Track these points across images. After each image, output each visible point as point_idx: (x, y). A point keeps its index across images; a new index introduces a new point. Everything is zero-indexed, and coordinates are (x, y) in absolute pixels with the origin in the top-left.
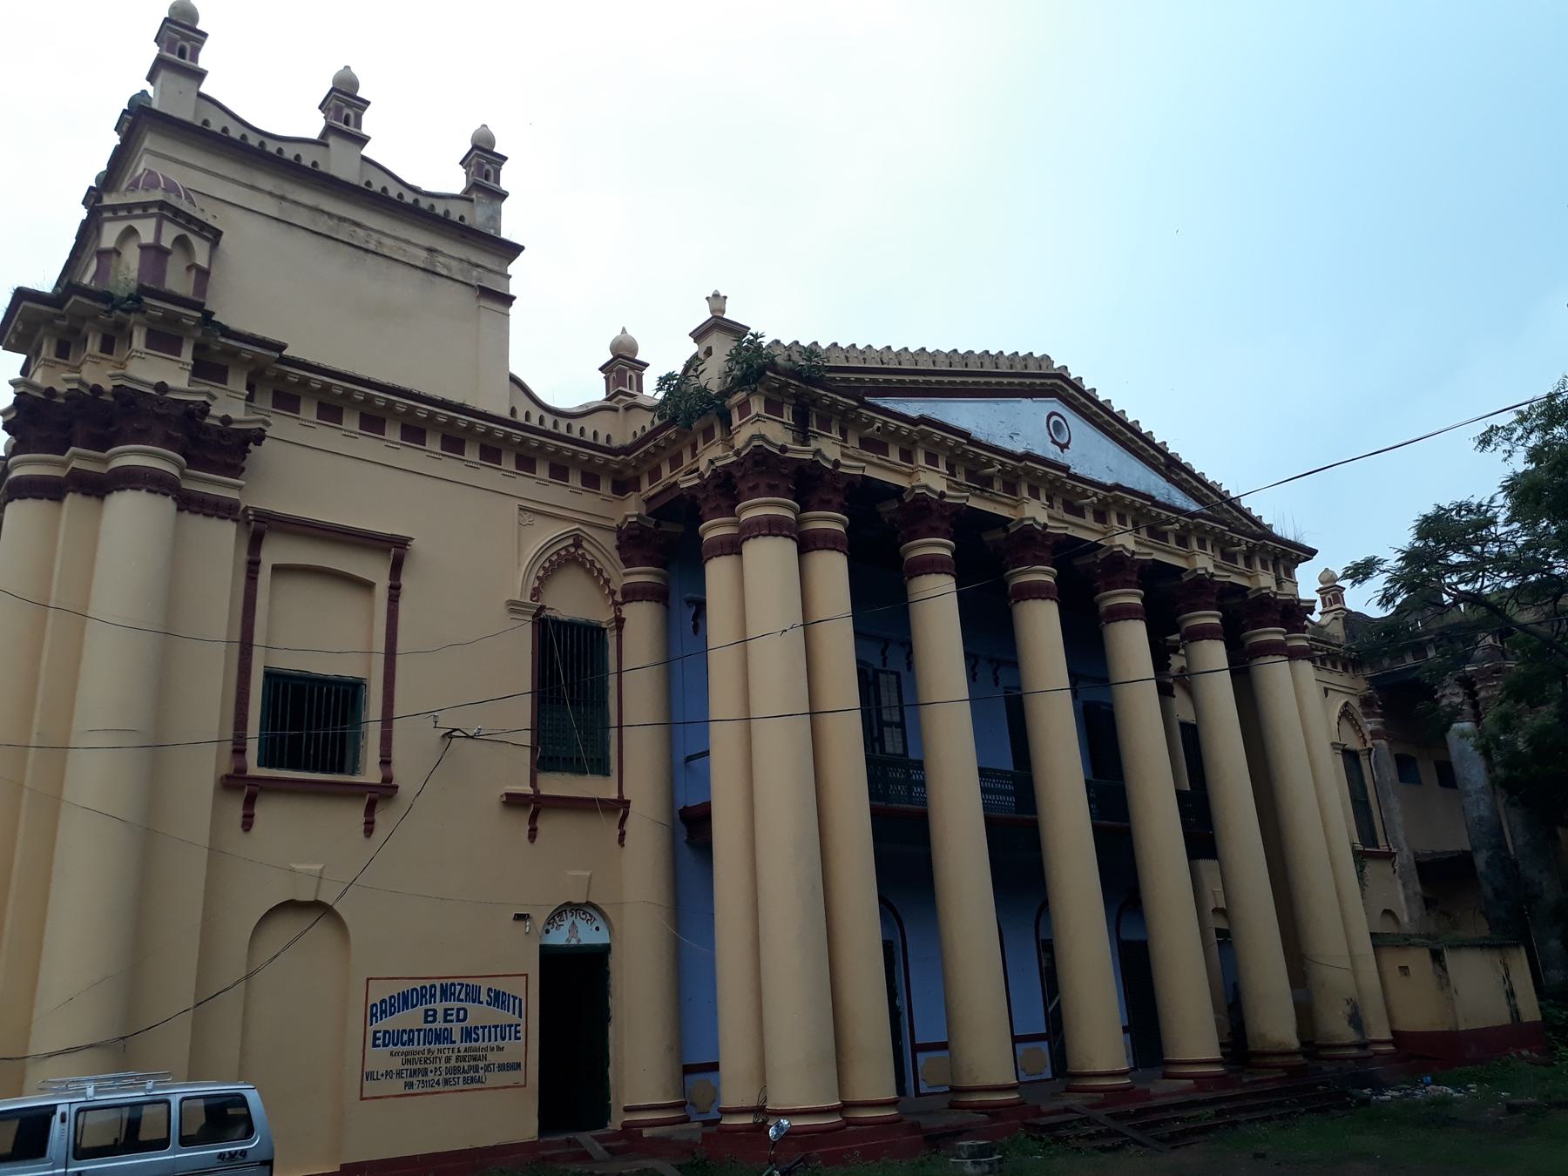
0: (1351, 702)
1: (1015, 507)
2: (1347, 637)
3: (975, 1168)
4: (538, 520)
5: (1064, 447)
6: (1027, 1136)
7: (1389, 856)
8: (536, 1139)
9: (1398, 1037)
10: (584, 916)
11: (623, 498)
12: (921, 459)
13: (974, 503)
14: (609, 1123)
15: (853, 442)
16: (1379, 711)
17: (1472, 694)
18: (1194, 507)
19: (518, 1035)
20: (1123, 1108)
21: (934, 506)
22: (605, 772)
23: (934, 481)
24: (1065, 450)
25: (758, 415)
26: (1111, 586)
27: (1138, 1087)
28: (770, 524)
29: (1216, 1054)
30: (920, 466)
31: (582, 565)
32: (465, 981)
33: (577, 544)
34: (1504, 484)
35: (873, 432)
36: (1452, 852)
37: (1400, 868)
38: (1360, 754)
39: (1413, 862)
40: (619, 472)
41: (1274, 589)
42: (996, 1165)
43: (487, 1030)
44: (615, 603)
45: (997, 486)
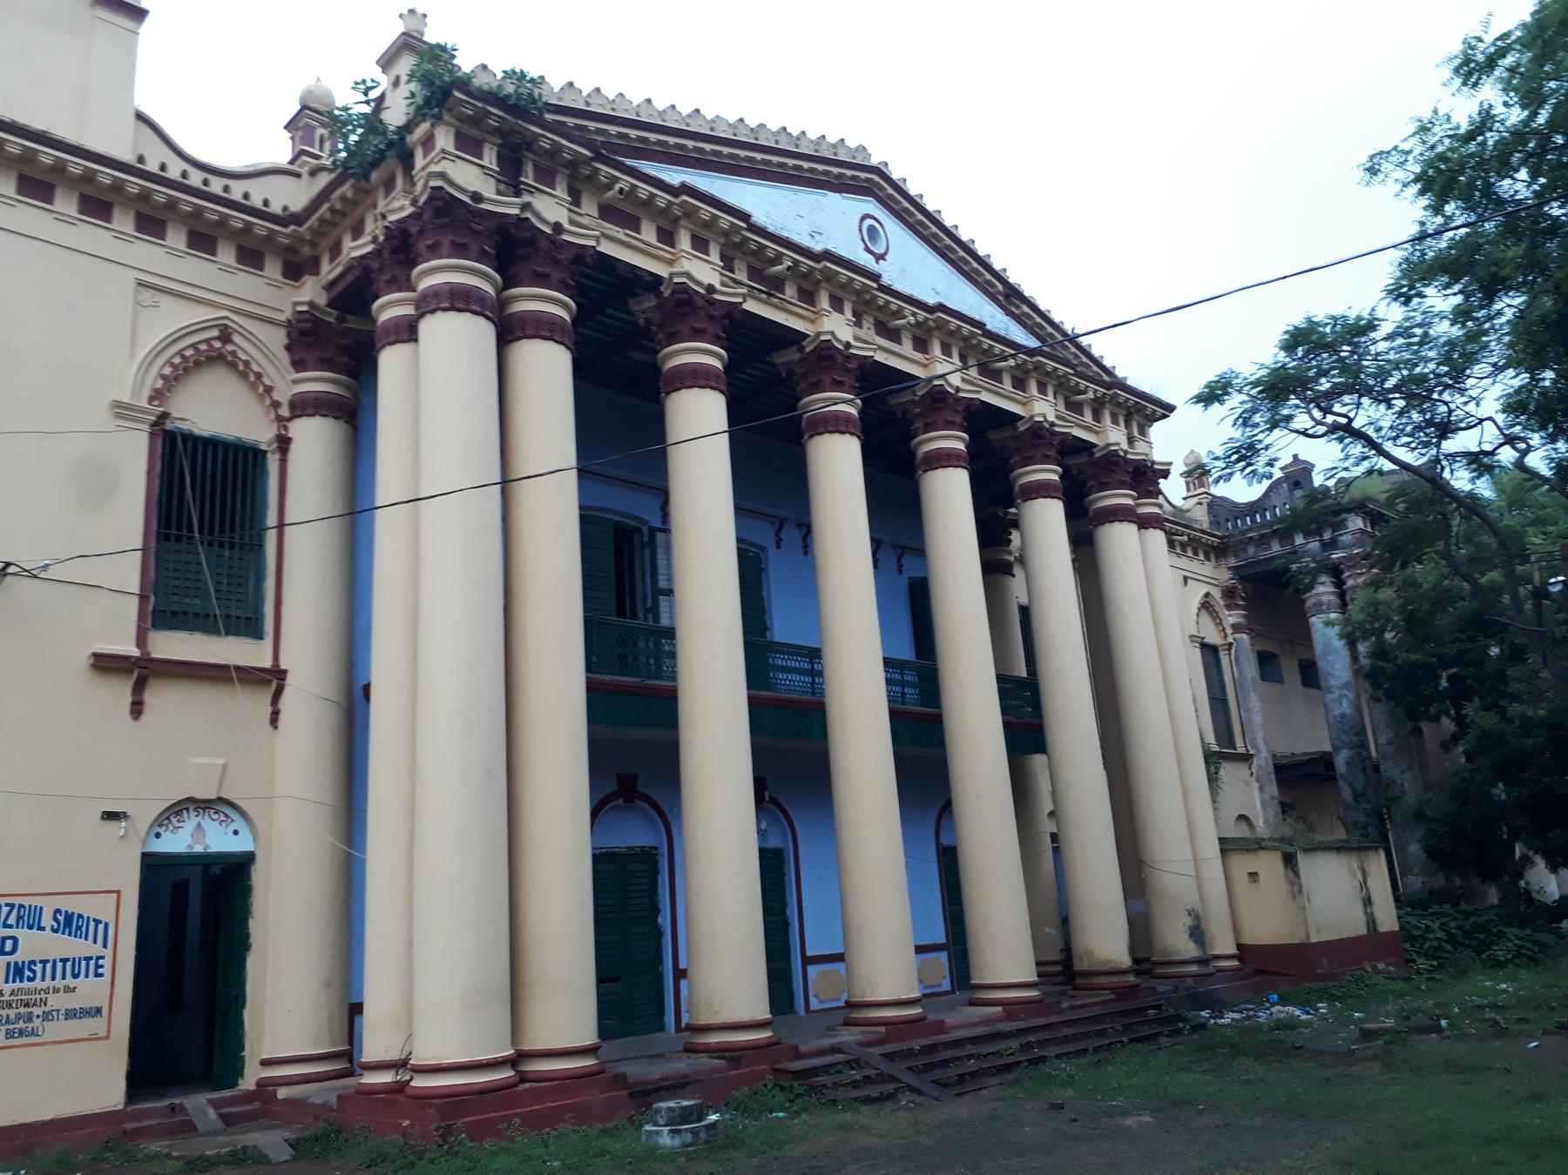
0: (1212, 593)
1: (813, 321)
2: (1211, 523)
3: (672, 1138)
4: (166, 302)
5: (880, 257)
6: (776, 1085)
7: (1246, 758)
8: (121, 1107)
9: (1243, 950)
10: (216, 816)
11: (296, 284)
12: (684, 242)
13: (751, 306)
14: (240, 1081)
15: (589, 207)
16: (1241, 603)
17: (1339, 584)
18: (1033, 343)
19: (100, 971)
20: (904, 1046)
21: (700, 302)
22: (258, 634)
23: (704, 271)
24: (881, 262)
25: (443, 151)
26: (930, 427)
27: (931, 1017)
28: (452, 295)
29: (1031, 977)
30: (683, 251)
31: (232, 366)
32: (17, 901)
33: (225, 337)
34: (1387, 288)
35: (613, 197)
36: (1312, 753)
37: (1257, 771)
38: (1220, 648)
39: (1270, 763)
40: (289, 249)
41: (1125, 446)
42: (703, 1135)
43: (49, 966)
44: (280, 419)
45: (790, 292)
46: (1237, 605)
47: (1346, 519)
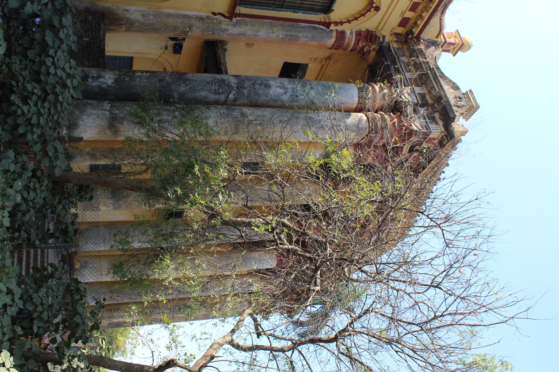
37: (217, 19)
46: (360, 40)
47: (437, 124)
